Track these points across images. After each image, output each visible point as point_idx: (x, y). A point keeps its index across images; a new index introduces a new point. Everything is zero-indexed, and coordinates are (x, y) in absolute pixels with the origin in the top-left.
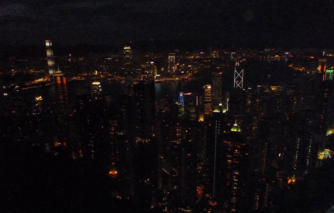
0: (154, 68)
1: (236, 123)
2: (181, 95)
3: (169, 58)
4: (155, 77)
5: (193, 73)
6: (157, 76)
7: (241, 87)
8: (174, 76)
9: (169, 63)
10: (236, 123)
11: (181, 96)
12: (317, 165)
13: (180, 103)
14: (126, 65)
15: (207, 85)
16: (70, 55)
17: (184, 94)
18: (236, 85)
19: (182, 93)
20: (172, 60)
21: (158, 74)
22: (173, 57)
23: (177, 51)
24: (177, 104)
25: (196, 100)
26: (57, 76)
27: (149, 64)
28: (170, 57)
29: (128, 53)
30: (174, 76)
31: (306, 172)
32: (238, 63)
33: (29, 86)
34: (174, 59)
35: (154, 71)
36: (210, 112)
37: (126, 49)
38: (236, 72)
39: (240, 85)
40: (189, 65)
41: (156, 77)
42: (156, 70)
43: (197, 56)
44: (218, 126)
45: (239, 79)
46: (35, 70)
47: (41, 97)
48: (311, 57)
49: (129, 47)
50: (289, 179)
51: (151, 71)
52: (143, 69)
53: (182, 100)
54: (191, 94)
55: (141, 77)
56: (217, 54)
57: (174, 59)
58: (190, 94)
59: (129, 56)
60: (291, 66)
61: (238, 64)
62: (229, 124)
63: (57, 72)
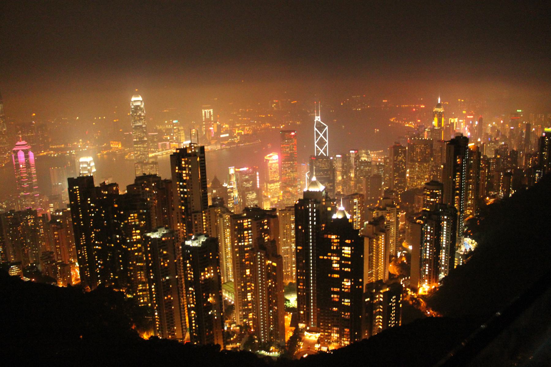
0: (179, 130)
1: (342, 205)
2: (232, 171)
3: (203, 112)
7: (326, 154)
8: (213, 142)
9: (204, 122)
10: (342, 205)
11: (232, 174)
12: (456, 263)
13: (232, 185)
14: (135, 126)
15: (271, 154)
16: (34, 114)
17: (237, 170)
18: (318, 152)
19: (233, 168)
20: (208, 116)
21: (186, 139)
22: (210, 112)
24: (226, 187)
26: (19, 150)
28: (205, 113)
31: (442, 276)
32: (319, 117)
34: (212, 114)
35: (180, 136)
36: (278, 197)
37: (135, 101)
38: (316, 131)
39: (325, 151)
42: (182, 133)
44: (313, 212)
45: (321, 143)
48: (422, 106)
49: (138, 96)
50: (420, 287)
51: (173, 136)
52: (160, 132)
53: (234, 179)
54: (248, 168)
57: (212, 114)
58: (245, 169)
60: (394, 120)
61: (319, 119)
62: (329, 209)
63: (18, 143)
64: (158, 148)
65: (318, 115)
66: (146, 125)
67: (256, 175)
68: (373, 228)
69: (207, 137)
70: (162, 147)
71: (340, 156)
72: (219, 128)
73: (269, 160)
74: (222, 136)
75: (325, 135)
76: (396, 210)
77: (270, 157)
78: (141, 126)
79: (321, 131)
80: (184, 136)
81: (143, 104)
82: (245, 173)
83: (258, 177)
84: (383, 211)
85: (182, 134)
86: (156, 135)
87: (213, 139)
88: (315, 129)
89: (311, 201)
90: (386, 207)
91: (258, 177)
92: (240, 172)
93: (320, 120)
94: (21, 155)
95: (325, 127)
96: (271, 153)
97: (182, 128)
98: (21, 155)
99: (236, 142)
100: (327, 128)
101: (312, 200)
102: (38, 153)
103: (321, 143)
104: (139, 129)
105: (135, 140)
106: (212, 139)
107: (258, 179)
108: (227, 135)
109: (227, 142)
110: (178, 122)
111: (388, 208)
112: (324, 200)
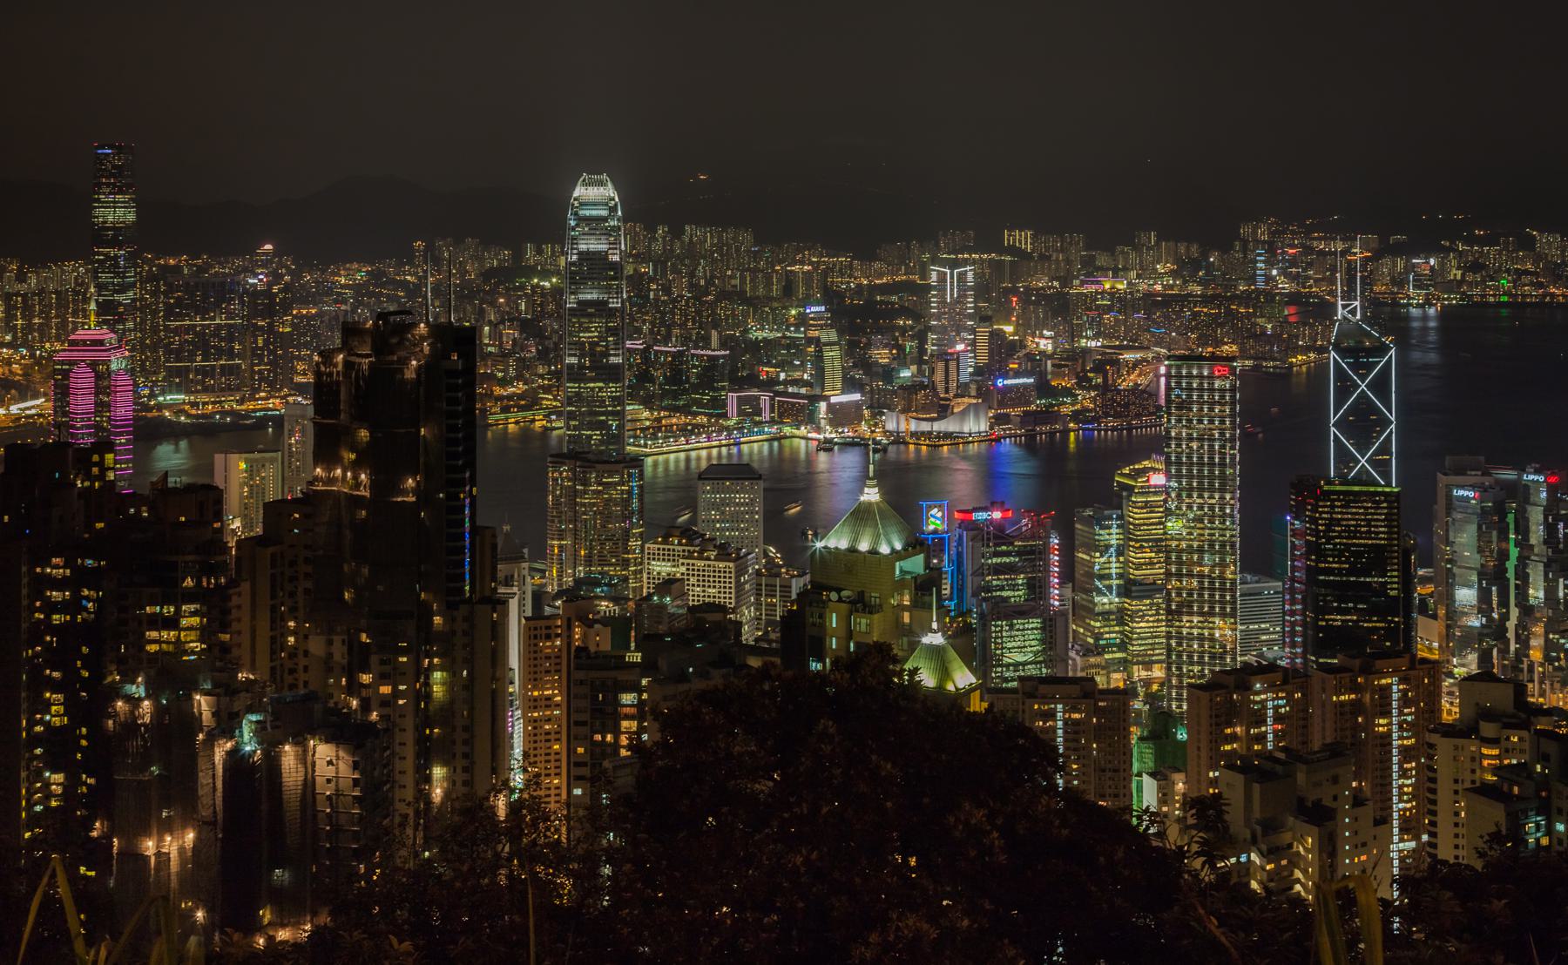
3: (934, 276)
4: (823, 406)
5: (1105, 389)
6: (833, 400)
8: (960, 405)
9: (938, 317)
11: (935, 532)
14: (580, 303)
15: (1146, 463)
16: (268, 247)
18: (1345, 458)
21: (850, 385)
22: (962, 276)
23: (1023, 239)
25: (1047, 564)
26: (72, 363)
27: (802, 320)
40: (1087, 338)
41: (831, 408)
43: (1161, 276)
45: (1363, 424)
55: (724, 405)
59: (604, 247)
64: (725, 416)
66: (622, 302)
67: (1044, 552)
69: (940, 387)
70: (741, 413)
71: (1471, 494)
72: (1002, 351)
73: (1130, 489)
74: (1000, 383)
76: (1526, 746)
78: (600, 306)
79: (1362, 368)
80: (839, 375)
81: (620, 213)
82: (999, 535)
84: (1460, 742)
85: (827, 365)
86: (723, 357)
87: (963, 391)
90: (1477, 723)
94: (83, 380)
95: (1383, 350)
96: (1148, 458)
97: (833, 335)
98: (83, 380)
102: (241, 402)
103: (1363, 424)
104: (590, 315)
105: (574, 360)
106: (956, 396)
109: (1018, 411)
110: (827, 310)
111: (1488, 729)
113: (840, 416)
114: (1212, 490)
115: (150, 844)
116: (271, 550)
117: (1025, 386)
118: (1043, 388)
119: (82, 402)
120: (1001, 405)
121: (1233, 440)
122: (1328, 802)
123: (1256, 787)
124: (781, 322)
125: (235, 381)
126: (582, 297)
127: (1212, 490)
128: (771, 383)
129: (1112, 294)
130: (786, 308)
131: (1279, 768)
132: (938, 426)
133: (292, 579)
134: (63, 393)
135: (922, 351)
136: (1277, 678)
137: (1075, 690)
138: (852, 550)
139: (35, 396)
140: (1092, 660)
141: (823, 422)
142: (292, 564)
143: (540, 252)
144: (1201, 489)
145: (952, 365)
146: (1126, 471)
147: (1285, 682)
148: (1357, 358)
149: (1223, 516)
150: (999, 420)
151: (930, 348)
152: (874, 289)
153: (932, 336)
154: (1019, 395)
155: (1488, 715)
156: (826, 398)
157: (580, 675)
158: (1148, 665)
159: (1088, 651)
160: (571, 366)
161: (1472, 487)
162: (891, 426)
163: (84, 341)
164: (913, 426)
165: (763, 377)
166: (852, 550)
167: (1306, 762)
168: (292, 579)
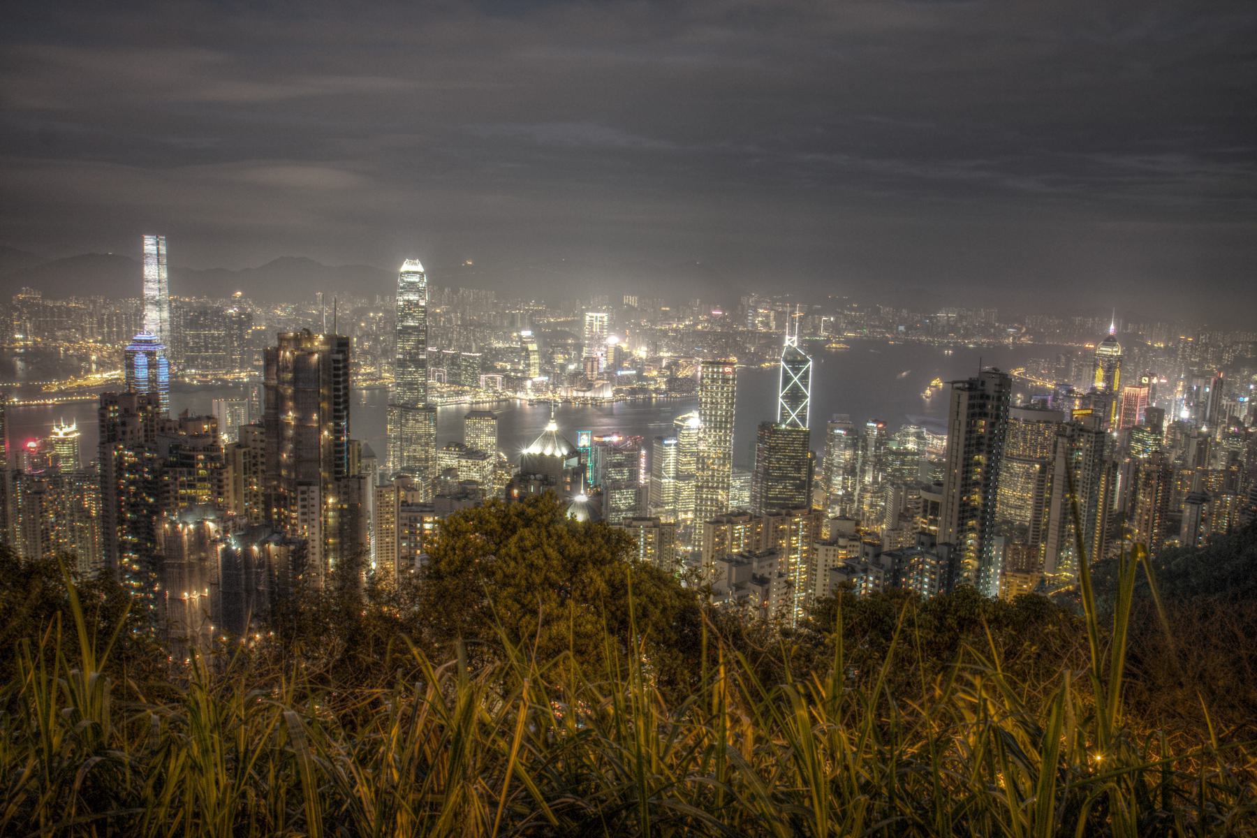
1: (582, 492)
3: (588, 318)
8: (598, 384)
10: (582, 492)
11: (584, 447)
14: (403, 327)
16: (239, 293)
20: (596, 329)
21: (543, 372)
29: (412, 287)
30: (598, 384)
32: (795, 338)
33: (61, 393)
37: (408, 273)
39: (803, 419)
41: (534, 384)
43: (701, 322)
45: (795, 397)
46: (101, 342)
47: (74, 427)
51: (519, 363)
56: (772, 318)
61: (793, 342)
65: (792, 334)
67: (639, 456)
68: (730, 570)
70: (487, 384)
71: (842, 432)
73: (681, 427)
74: (619, 373)
75: (804, 378)
77: (684, 420)
83: (643, 460)
88: (782, 363)
89: (535, 479)
91: (643, 460)
92: (603, 444)
93: (796, 345)
94: (141, 360)
99: (652, 387)
100: (811, 363)
101: (537, 476)
102: (226, 374)
103: (795, 397)
105: (401, 356)
106: (597, 379)
107: (643, 465)
108: (634, 372)
109: (628, 387)
112: (569, 480)
113: (537, 388)
114: (721, 428)
115: (186, 594)
116: (243, 450)
117: (632, 375)
118: (640, 377)
119: (142, 374)
120: (619, 384)
121: (732, 404)
122: (767, 575)
123: (734, 569)
124: (507, 338)
125: (220, 363)
126: (405, 324)
127: (721, 428)
128: (503, 370)
129: (676, 331)
130: (511, 332)
131: (745, 560)
132: (588, 394)
133: (255, 465)
134: (130, 366)
135: (580, 356)
136: (747, 518)
137: (650, 523)
138: (542, 454)
139: (116, 369)
140: (659, 509)
141: (529, 391)
142: (255, 457)
143: (383, 300)
144: (715, 428)
145: (595, 364)
146: (680, 418)
147: (751, 520)
148: (793, 365)
149: (726, 441)
150: (618, 392)
151: (584, 355)
152: (557, 324)
153: (585, 349)
154: (627, 380)
155: (842, 535)
156: (531, 379)
157: (404, 515)
158: (686, 512)
159: (657, 505)
160: (399, 359)
161: (844, 429)
162: (563, 394)
163: (141, 341)
164: (575, 394)
165: (499, 367)
166: (542, 454)
167: (758, 557)
168: (255, 465)
